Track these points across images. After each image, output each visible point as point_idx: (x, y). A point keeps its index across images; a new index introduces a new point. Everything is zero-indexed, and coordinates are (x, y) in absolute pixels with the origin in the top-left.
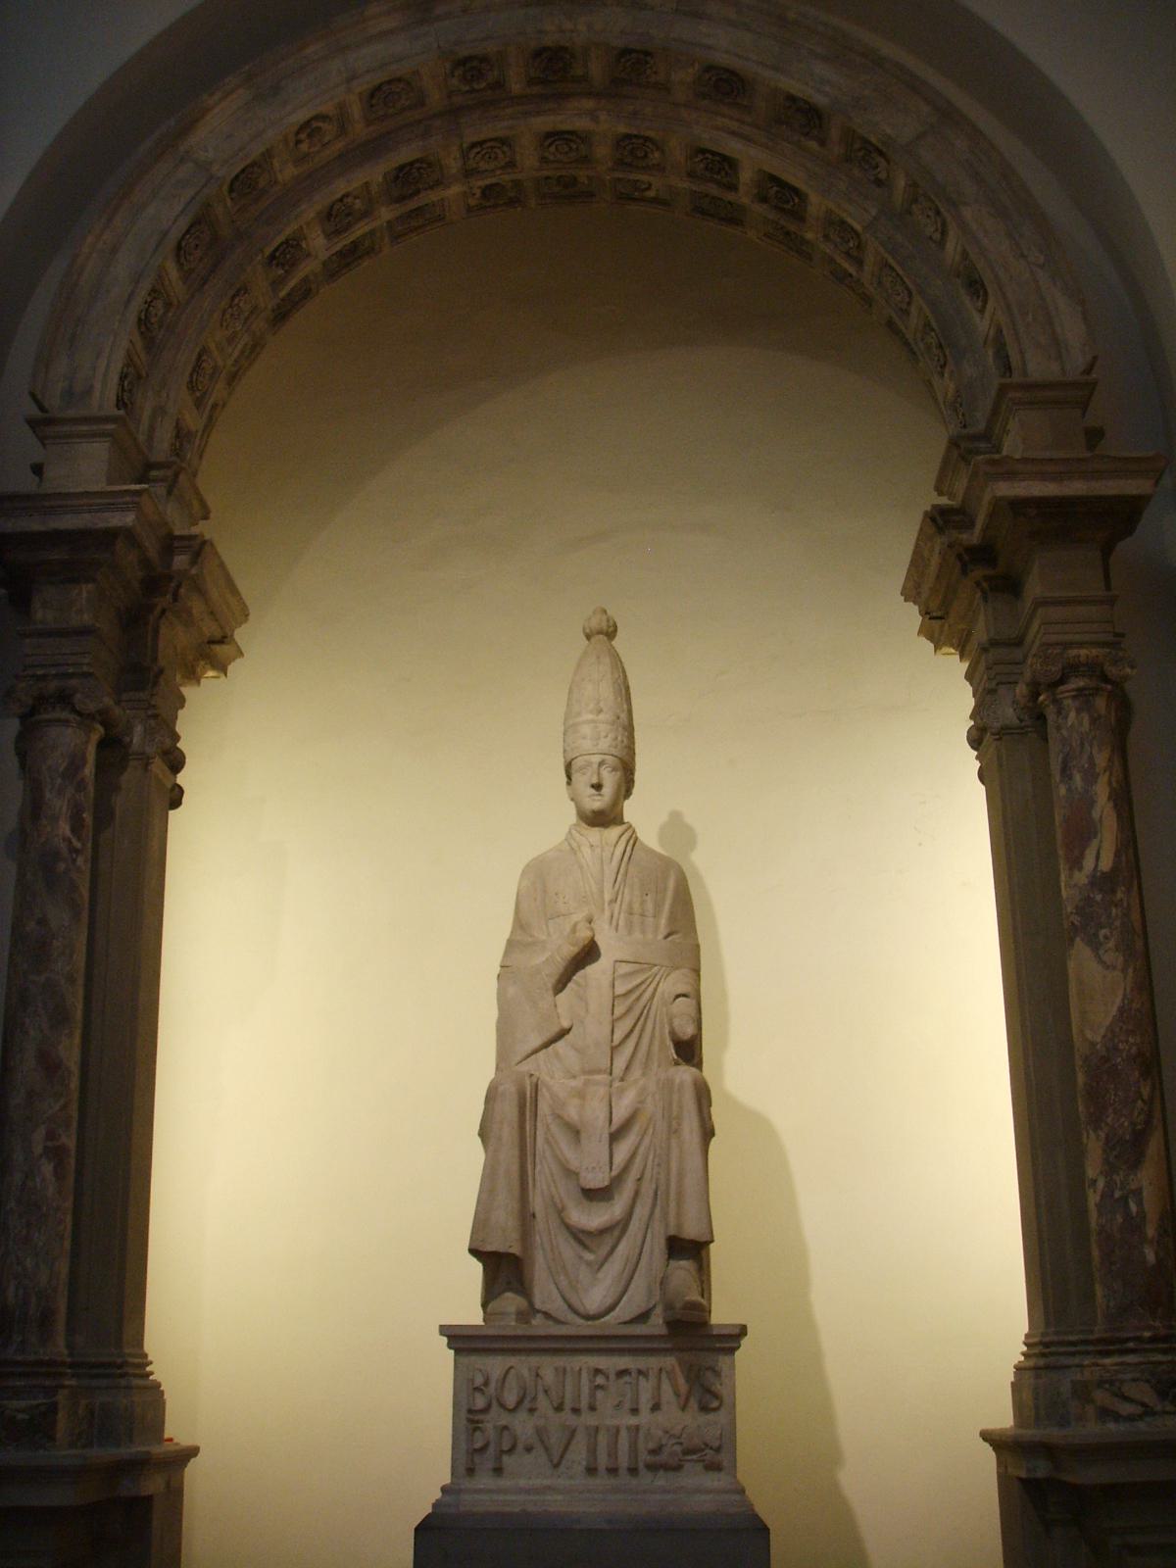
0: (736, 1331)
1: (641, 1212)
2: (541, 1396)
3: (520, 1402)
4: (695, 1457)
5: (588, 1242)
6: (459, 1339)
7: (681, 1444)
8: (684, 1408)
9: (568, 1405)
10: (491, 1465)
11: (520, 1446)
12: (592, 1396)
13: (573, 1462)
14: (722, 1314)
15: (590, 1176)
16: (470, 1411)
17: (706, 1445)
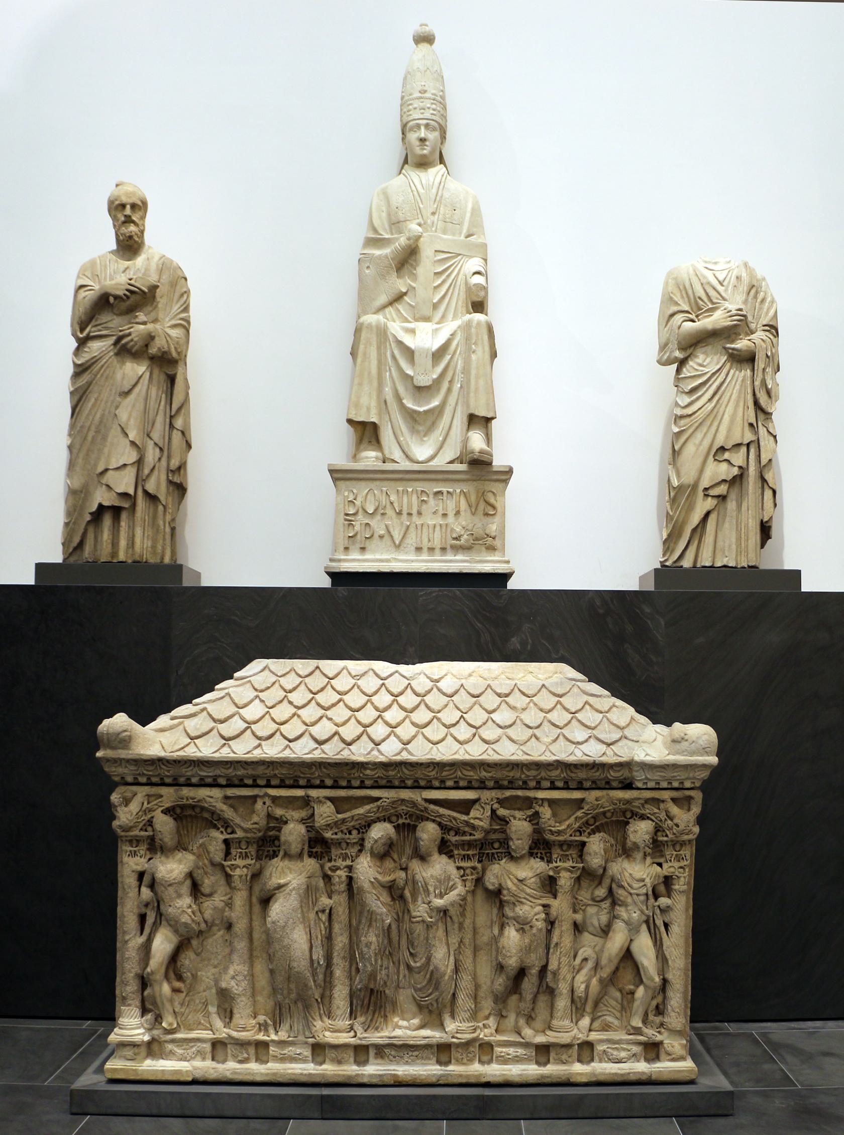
0: (507, 470)
1: (452, 401)
3: (376, 510)
4: (480, 542)
5: (417, 419)
6: (338, 475)
8: (473, 514)
9: (405, 512)
10: (358, 546)
11: (376, 536)
12: (419, 506)
14: (499, 462)
16: (347, 515)
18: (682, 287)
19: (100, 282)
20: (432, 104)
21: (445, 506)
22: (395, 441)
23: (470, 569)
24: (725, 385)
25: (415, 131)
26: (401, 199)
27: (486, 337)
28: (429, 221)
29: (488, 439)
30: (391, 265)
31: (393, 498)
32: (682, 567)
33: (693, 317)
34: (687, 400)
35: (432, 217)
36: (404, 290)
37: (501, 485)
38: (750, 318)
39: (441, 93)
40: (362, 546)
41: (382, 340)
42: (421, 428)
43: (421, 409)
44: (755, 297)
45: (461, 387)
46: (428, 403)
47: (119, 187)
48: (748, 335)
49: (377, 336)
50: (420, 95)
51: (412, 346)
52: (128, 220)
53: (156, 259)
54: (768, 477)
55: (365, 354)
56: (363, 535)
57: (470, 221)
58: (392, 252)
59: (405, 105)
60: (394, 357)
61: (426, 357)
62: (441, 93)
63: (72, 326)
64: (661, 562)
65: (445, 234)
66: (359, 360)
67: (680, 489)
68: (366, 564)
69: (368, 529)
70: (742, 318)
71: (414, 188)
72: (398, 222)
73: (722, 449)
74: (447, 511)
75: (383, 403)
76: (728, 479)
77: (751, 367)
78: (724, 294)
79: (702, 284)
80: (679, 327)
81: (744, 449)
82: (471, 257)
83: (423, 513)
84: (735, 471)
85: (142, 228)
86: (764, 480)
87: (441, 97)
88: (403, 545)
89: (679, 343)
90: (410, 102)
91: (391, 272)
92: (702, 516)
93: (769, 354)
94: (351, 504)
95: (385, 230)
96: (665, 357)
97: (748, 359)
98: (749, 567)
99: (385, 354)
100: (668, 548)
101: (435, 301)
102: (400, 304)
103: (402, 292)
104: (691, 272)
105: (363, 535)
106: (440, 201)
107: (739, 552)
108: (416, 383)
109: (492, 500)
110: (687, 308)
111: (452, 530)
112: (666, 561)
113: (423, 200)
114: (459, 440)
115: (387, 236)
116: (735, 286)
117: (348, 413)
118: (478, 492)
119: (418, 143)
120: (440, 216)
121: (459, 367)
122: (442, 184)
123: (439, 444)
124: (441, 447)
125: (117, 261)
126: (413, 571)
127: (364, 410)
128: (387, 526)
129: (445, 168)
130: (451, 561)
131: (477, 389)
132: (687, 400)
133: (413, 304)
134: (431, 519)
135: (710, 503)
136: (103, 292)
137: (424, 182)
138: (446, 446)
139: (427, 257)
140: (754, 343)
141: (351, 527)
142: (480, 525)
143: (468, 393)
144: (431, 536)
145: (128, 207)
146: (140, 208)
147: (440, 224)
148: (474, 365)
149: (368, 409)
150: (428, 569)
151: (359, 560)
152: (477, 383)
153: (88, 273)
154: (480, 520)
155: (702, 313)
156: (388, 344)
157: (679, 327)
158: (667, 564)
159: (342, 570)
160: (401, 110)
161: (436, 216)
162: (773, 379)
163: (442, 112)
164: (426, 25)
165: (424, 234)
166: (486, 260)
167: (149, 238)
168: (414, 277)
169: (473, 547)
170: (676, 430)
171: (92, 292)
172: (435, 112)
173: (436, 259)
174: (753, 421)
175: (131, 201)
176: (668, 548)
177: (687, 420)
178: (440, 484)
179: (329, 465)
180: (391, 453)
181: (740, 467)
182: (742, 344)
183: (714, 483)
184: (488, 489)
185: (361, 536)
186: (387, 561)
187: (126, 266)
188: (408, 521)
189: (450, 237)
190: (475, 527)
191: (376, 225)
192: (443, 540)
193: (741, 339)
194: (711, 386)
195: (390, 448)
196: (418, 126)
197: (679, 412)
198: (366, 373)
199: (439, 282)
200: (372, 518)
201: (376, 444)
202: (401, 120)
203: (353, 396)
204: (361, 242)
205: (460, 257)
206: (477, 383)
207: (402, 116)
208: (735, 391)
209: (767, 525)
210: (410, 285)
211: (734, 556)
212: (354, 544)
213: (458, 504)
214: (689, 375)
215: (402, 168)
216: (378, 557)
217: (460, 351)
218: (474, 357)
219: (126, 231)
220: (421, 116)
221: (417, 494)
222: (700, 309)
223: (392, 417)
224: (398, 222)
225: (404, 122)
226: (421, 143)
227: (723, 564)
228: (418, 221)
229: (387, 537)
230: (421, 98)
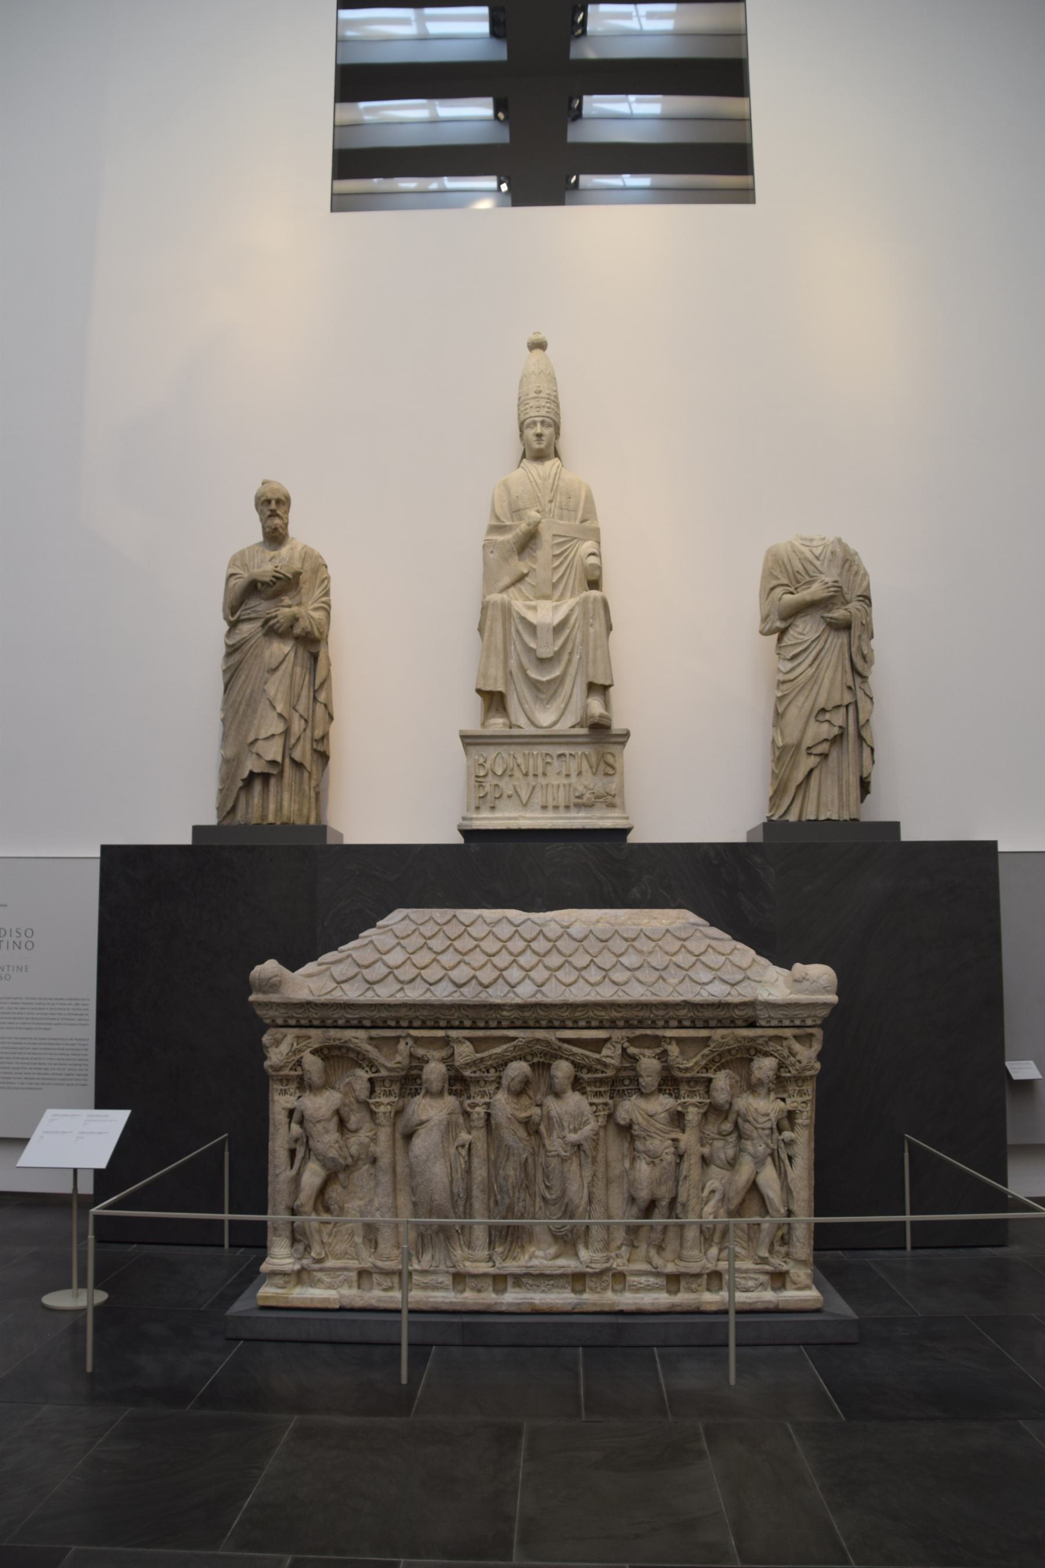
0: (625, 732)
2: (516, 768)
3: (504, 772)
4: (601, 800)
5: (541, 688)
7: (594, 793)
8: (594, 774)
9: (531, 773)
10: (489, 805)
11: (505, 795)
16: (477, 777)
17: (608, 794)
18: (781, 563)
19: (248, 571)
20: (547, 402)
22: (520, 709)
24: (824, 652)
27: (602, 612)
28: (547, 509)
29: (607, 705)
30: (513, 549)
31: (520, 760)
32: (787, 821)
33: (792, 589)
34: (789, 665)
36: (525, 571)
37: (619, 747)
38: (845, 590)
39: (555, 393)
40: (492, 805)
42: (543, 696)
43: (544, 679)
44: (849, 570)
45: (580, 658)
47: (265, 485)
48: (843, 604)
50: (535, 395)
52: (273, 514)
53: (299, 548)
54: (864, 734)
55: (491, 629)
57: (584, 508)
59: (522, 405)
60: (517, 631)
62: (555, 393)
63: (224, 610)
64: (768, 817)
66: (486, 634)
67: (784, 749)
68: (496, 822)
70: (838, 589)
73: (823, 710)
76: (830, 739)
77: (847, 634)
78: (820, 568)
79: (800, 559)
80: (780, 599)
81: (843, 710)
82: (585, 540)
83: (548, 774)
84: (836, 731)
85: (286, 521)
86: (861, 739)
89: (780, 614)
90: (527, 402)
92: (806, 773)
93: (864, 622)
96: (767, 628)
97: (845, 627)
98: (852, 820)
100: (774, 804)
101: (554, 581)
104: (789, 549)
106: (556, 490)
107: (841, 807)
110: (786, 582)
111: (575, 789)
112: (773, 815)
115: (508, 523)
116: (830, 560)
117: (477, 684)
119: (535, 438)
121: (578, 640)
122: (558, 474)
124: (562, 714)
125: (263, 551)
128: (515, 787)
129: (559, 461)
130: (574, 818)
132: (789, 665)
135: (812, 761)
136: (251, 579)
138: (567, 712)
140: (850, 612)
141: (481, 788)
142: (600, 785)
144: (555, 795)
145: (273, 502)
146: (284, 503)
147: (557, 511)
149: (496, 680)
151: (489, 819)
153: (238, 563)
155: (801, 586)
157: (780, 599)
158: (775, 818)
159: (474, 828)
160: (519, 409)
161: (553, 504)
162: (869, 646)
163: (556, 410)
164: (539, 333)
165: (543, 521)
166: (599, 543)
167: (293, 530)
168: (534, 559)
170: (780, 694)
171: (241, 580)
172: (549, 410)
174: (851, 684)
175: (276, 497)
176: (774, 804)
177: (790, 685)
181: (840, 727)
182: (839, 613)
183: (816, 742)
186: (515, 818)
187: (272, 555)
189: (567, 523)
190: (596, 786)
191: (498, 514)
193: (838, 609)
194: (810, 652)
196: (535, 423)
197: (782, 677)
199: (557, 563)
202: (519, 419)
204: (485, 529)
207: (519, 415)
208: (833, 657)
209: (866, 780)
211: (837, 810)
214: (790, 643)
215: (521, 461)
216: (507, 815)
218: (591, 630)
219: (271, 524)
220: (537, 414)
222: (798, 582)
223: (518, 687)
225: (522, 419)
227: (826, 818)
228: (536, 508)
229: (515, 797)
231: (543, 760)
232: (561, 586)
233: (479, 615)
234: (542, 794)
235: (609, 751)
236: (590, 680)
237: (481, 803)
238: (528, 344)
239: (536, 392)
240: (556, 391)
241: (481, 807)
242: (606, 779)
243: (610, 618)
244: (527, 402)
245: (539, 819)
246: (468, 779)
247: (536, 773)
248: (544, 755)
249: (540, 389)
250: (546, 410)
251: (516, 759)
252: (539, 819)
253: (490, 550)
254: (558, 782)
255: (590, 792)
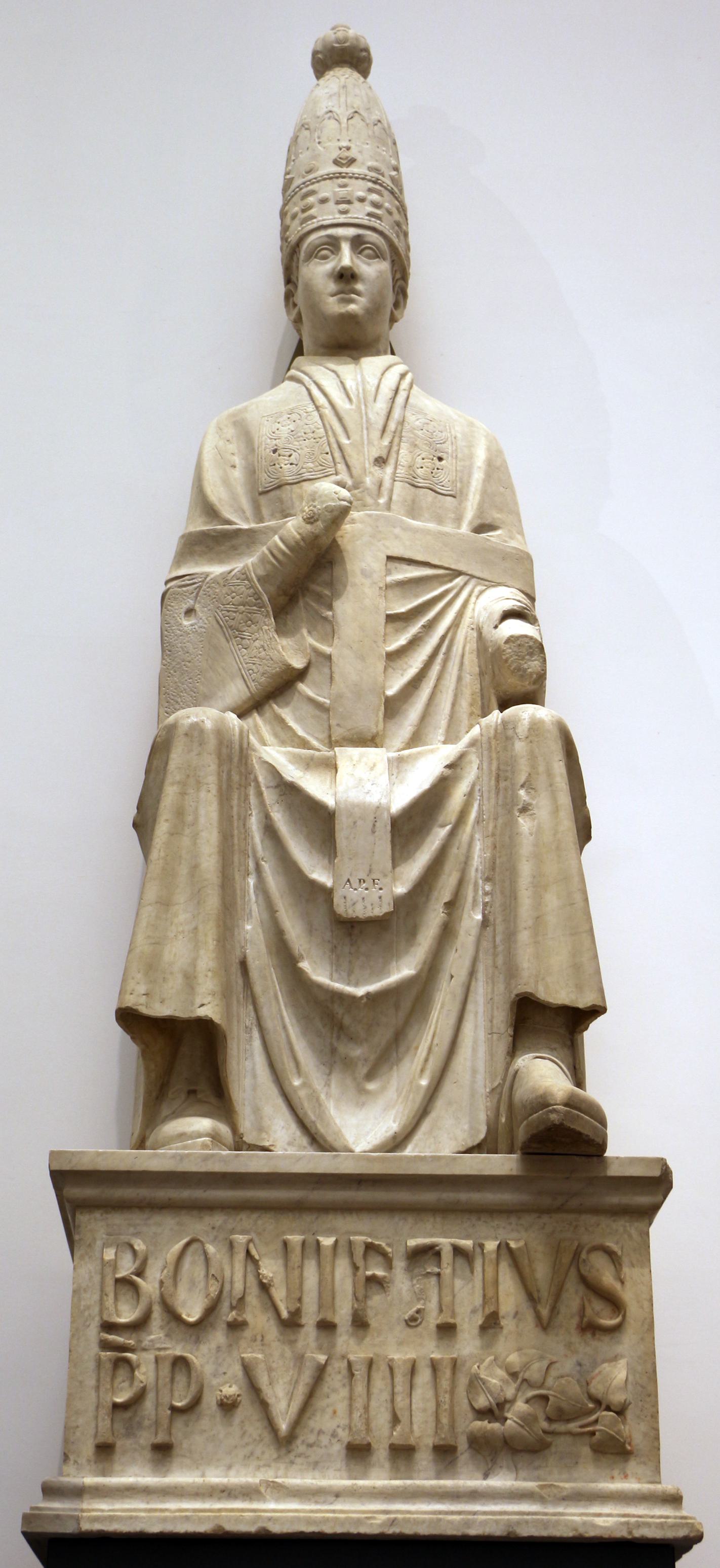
0: (657, 1173)
2: (253, 1299)
3: (211, 1311)
4: (573, 1426)
5: (347, 1021)
7: (545, 1398)
8: (544, 1325)
9: (310, 1318)
10: (146, 1438)
11: (210, 1401)
13: (320, 1432)
15: (353, 894)
16: (109, 1327)
17: (598, 1402)
20: (370, 190)
21: (447, 1299)
22: (273, 1091)
23: (546, 1524)
25: (325, 258)
26: (284, 431)
27: (559, 768)
28: (368, 481)
29: (578, 1076)
30: (258, 597)
31: (270, 1268)
35: (376, 471)
36: (298, 663)
37: (633, 1228)
39: (394, 173)
40: (161, 1438)
41: (236, 778)
42: (357, 1052)
43: (360, 991)
45: (485, 923)
46: (382, 972)
49: (219, 756)
51: (330, 802)
55: (180, 813)
56: (165, 1399)
57: (484, 493)
58: (263, 560)
59: (297, 198)
60: (270, 830)
61: (373, 832)
65: (413, 519)
66: (162, 829)
68: (172, 1505)
69: (181, 1379)
71: (322, 400)
72: (279, 487)
74: (453, 1315)
75: (235, 969)
83: (373, 1323)
87: (392, 179)
88: (306, 1436)
90: (311, 188)
91: (258, 616)
94: (125, 1291)
95: (241, 511)
99: (244, 820)
101: (390, 692)
102: (287, 704)
103: (289, 668)
105: (165, 1399)
106: (398, 434)
108: (341, 907)
109: (608, 1279)
111: (475, 1383)
113: (351, 426)
114: (483, 1086)
115: (245, 526)
117: (122, 992)
118: (556, 1250)
119: (332, 286)
120: (401, 471)
121: (476, 861)
123: (418, 1099)
124: (423, 1112)
126: (339, 1530)
127: (176, 983)
128: (247, 1369)
130: (474, 1495)
131: (538, 920)
133: (328, 701)
134: (400, 1343)
137: (350, 384)
138: (440, 1104)
139: (365, 574)
141: (122, 1373)
142: (568, 1366)
143: (511, 936)
144: (401, 1402)
148: (526, 847)
149: (190, 980)
150: (393, 1522)
151: (146, 1492)
152: (538, 902)
154: (569, 1345)
156: (252, 792)
159: (86, 1526)
161: (389, 470)
163: (397, 217)
168: (328, 629)
169: (547, 1446)
173: (389, 579)
178: (429, 1223)
179: (52, 1154)
180: (261, 1129)
184: (589, 1240)
185: (157, 1405)
186: (249, 1493)
188: (320, 1348)
189: (431, 526)
190: (553, 1373)
192: (445, 1420)
195: (257, 1110)
196: (334, 244)
198: (183, 871)
199: (402, 640)
200: (198, 1341)
201: (213, 1100)
202: (284, 239)
203: (140, 938)
204: (171, 546)
205: (459, 581)
206: (538, 902)
210: (315, 651)
212: (130, 1431)
213: (490, 1293)
216: (215, 1478)
217: (480, 812)
218: (524, 824)
220: (342, 219)
221: (351, 1255)
223: (265, 1012)
224: (279, 487)
225: (293, 238)
226: (342, 286)
229: (247, 1410)
230: (340, 176)
231: (356, 1268)
232: (414, 712)
233: (143, 777)
234: (351, 1398)
235: (598, 1241)
236: (522, 989)
237: (118, 1426)
238: (315, 53)
239: (336, 162)
240: (396, 169)
241: (119, 1444)
242: (587, 1347)
243: (583, 797)
244: (311, 188)
245: (338, 1495)
246: (75, 1334)
247: (329, 1317)
248: (359, 1251)
249: (353, 153)
250: (370, 209)
251: (256, 1263)
252: (338, 1495)
253: (185, 607)
254: (412, 1355)
255: (531, 1393)
